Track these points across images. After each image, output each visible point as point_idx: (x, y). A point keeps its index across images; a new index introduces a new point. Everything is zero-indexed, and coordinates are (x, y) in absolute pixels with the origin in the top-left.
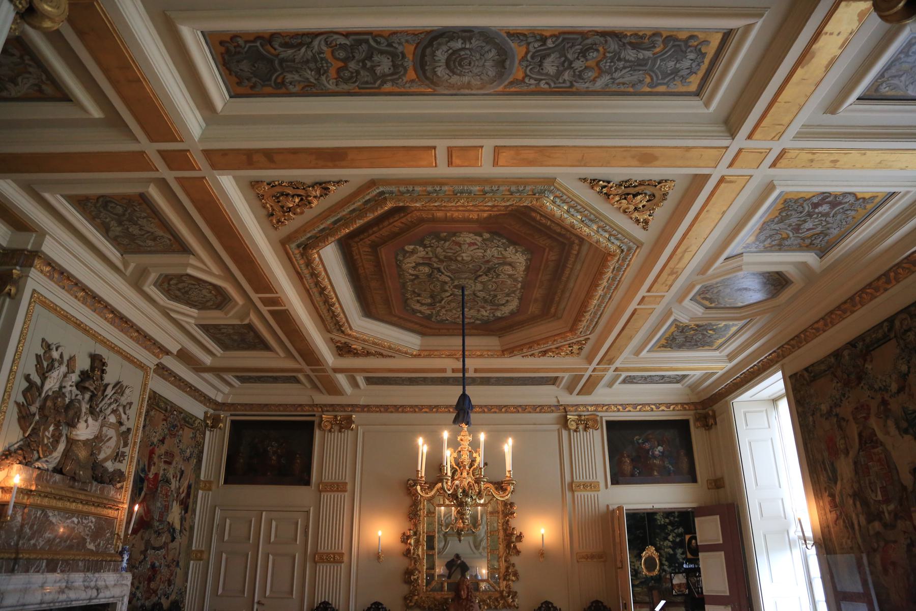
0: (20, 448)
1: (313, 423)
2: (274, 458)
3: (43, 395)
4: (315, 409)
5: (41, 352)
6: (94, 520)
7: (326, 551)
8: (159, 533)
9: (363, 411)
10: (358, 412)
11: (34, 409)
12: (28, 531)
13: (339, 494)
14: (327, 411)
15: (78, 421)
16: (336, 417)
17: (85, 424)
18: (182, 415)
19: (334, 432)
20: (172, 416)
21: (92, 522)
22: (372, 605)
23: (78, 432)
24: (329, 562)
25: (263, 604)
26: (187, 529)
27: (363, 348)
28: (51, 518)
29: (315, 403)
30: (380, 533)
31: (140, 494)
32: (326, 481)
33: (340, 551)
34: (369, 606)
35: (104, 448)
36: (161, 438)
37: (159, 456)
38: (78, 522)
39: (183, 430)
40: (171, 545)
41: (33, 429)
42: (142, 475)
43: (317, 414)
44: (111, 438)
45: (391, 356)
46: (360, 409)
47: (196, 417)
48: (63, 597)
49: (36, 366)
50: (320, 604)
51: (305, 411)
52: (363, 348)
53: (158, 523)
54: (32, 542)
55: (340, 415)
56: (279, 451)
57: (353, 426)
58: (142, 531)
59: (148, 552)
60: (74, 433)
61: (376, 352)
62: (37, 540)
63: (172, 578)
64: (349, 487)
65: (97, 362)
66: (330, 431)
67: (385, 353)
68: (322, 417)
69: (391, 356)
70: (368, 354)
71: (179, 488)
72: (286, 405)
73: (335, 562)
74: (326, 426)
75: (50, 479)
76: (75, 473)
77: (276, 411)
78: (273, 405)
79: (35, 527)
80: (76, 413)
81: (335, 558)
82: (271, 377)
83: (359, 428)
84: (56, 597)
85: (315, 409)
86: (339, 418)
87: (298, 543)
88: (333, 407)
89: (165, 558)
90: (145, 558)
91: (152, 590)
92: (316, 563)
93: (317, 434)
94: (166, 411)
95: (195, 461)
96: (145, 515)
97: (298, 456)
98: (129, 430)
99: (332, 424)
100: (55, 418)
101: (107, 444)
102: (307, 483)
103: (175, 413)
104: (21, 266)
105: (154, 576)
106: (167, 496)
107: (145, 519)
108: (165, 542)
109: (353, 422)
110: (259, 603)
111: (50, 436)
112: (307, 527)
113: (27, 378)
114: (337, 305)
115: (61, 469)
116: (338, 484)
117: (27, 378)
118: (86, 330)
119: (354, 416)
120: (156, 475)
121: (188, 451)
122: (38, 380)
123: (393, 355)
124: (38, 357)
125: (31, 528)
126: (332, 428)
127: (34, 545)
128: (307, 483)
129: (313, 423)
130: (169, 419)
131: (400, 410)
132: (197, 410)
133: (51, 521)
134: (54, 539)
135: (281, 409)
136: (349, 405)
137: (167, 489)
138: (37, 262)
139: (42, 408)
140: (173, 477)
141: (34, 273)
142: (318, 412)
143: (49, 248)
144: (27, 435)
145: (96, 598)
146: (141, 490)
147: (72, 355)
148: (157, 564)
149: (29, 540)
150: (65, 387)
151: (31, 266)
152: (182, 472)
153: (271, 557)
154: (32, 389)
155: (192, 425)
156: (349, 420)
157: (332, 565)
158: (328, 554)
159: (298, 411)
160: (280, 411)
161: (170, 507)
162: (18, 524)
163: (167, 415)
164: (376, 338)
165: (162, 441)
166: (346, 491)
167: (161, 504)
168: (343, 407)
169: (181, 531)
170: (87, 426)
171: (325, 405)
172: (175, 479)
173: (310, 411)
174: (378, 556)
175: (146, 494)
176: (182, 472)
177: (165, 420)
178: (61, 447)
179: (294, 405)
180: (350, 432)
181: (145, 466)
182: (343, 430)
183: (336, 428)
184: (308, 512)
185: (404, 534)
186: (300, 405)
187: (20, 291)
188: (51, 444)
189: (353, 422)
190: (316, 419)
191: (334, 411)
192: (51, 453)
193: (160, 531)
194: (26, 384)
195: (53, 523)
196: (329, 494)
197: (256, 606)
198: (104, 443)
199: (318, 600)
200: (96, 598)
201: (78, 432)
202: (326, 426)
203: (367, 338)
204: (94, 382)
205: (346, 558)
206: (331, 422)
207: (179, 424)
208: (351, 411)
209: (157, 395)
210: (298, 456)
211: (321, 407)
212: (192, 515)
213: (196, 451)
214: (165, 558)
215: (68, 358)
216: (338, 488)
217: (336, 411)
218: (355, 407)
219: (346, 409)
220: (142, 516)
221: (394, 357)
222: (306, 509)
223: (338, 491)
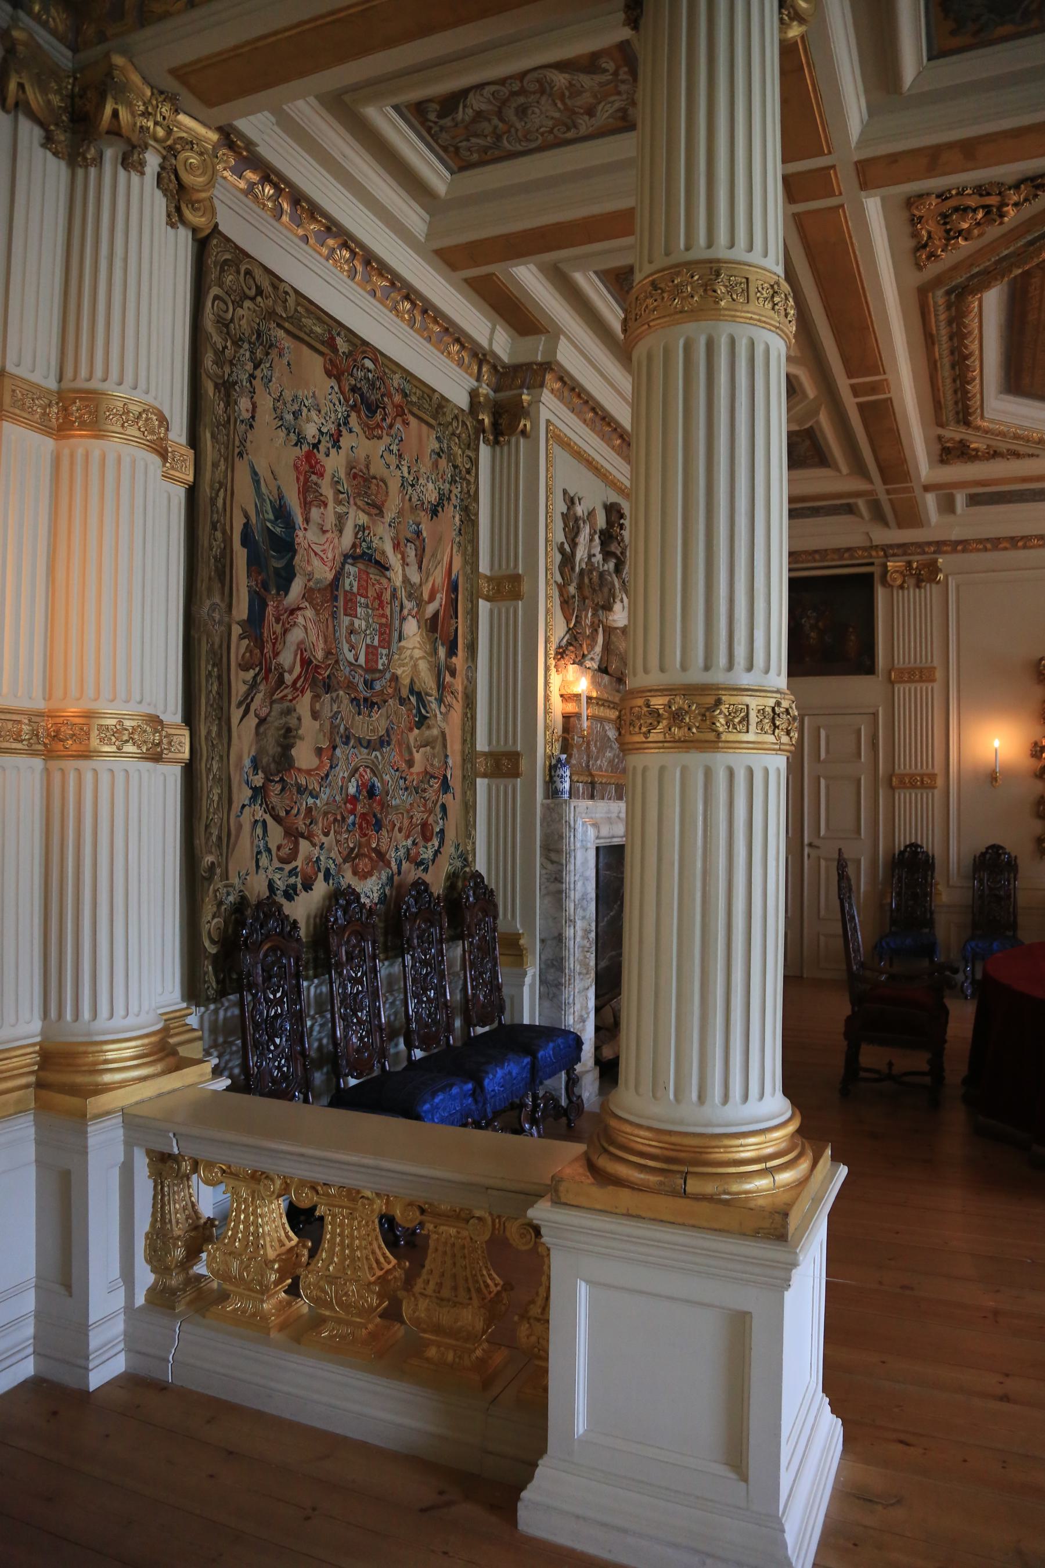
0: (569, 644)
1: (871, 575)
2: (812, 634)
3: (577, 569)
4: (874, 553)
7: (908, 770)
9: (954, 550)
10: (946, 552)
13: (924, 685)
14: (894, 555)
15: (614, 601)
16: (909, 564)
17: (621, 604)
19: (908, 588)
22: (987, 849)
23: (616, 617)
24: (914, 787)
25: (818, 847)
27: (988, 446)
29: (874, 543)
30: (997, 743)
32: (901, 665)
33: (930, 770)
34: (984, 850)
41: (577, 617)
43: (876, 561)
45: (1032, 455)
46: (949, 549)
49: (564, 529)
50: (906, 847)
51: (857, 559)
52: (988, 446)
55: (916, 560)
56: (820, 624)
57: (941, 576)
60: (610, 618)
61: (1008, 450)
62: (601, 761)
64: (939, 674)
66: (901, 587)
67: (1022, 450)
68: (886, 566)
69: (1032, 455)
70: (995, 454)
72: (826, 550)
73: (923, 786)
74: (895, 580)
76: (622, 673)
77: (808, 561)
78: (805, 552)
80: (610, 590)
81: (922, 782)
82: (809, 508)
83: (950, 579)
85: (874, 553)
86: (915, 565)
87: (863, 759)
88: (904, 548)
92: (892, 788)
93: (881, 594)
97: (851, 630)
99: (904, 576)
100: (593, 600)
102: (869, 669)
104: (528, 389)
109: (941, 571)
110: (810, 845)
112: (874, 737)
114: (977, 381)
115: (606, 668)
116: (921, 670)
119: (940, 560)
123: (1036, 452)
126: (904, 582)
128: (869, 669)
129: (871, 575)
131: (1020, 544)
135: (817, 557)
136: (929, 544)
138: (548, 377)
139: (580, 587)
141: (547, 396)
142: (878, 557)
143: (567, 356)
144: (572, 626)
147: (590, 510)
150: (594, 555)
151: (542, 385)
153: (823, 782)
156: (933, 569)
157: (919, 792)
158: (912, 776)
159: (846, 559)
160: (815, 561)
164: (1021, 427)
166: (933, 681)
168: (920, 547)
171: (891, 546)
173: (864, 558)
174: (992, 777)
179: (839, 550)
180: (934, 586)
182: (924, 584)
183: (912, 581)
184: (875, 715)
185: (1036, 744)
186: (848, 549)
187: (535, 425)
189: (941, 571)
190: (876, 570)
191: (905, 554)
196: (907, 686)
197: (806, 850)
199: (902, 841)
201: (616, 617)
202: (895, 580)
203: (1006, 429)
204: (619, 544)
205: (940, 782)
206: (902, 573)
208: (935, 552)
210: (851, 630)
211: (883, 550)
216: (921, 677)
217: (910, 555)
218: (939, 546)
219: (927, 549)
221: (1038, 456)
222: (871, 710)
223: (921, 680)
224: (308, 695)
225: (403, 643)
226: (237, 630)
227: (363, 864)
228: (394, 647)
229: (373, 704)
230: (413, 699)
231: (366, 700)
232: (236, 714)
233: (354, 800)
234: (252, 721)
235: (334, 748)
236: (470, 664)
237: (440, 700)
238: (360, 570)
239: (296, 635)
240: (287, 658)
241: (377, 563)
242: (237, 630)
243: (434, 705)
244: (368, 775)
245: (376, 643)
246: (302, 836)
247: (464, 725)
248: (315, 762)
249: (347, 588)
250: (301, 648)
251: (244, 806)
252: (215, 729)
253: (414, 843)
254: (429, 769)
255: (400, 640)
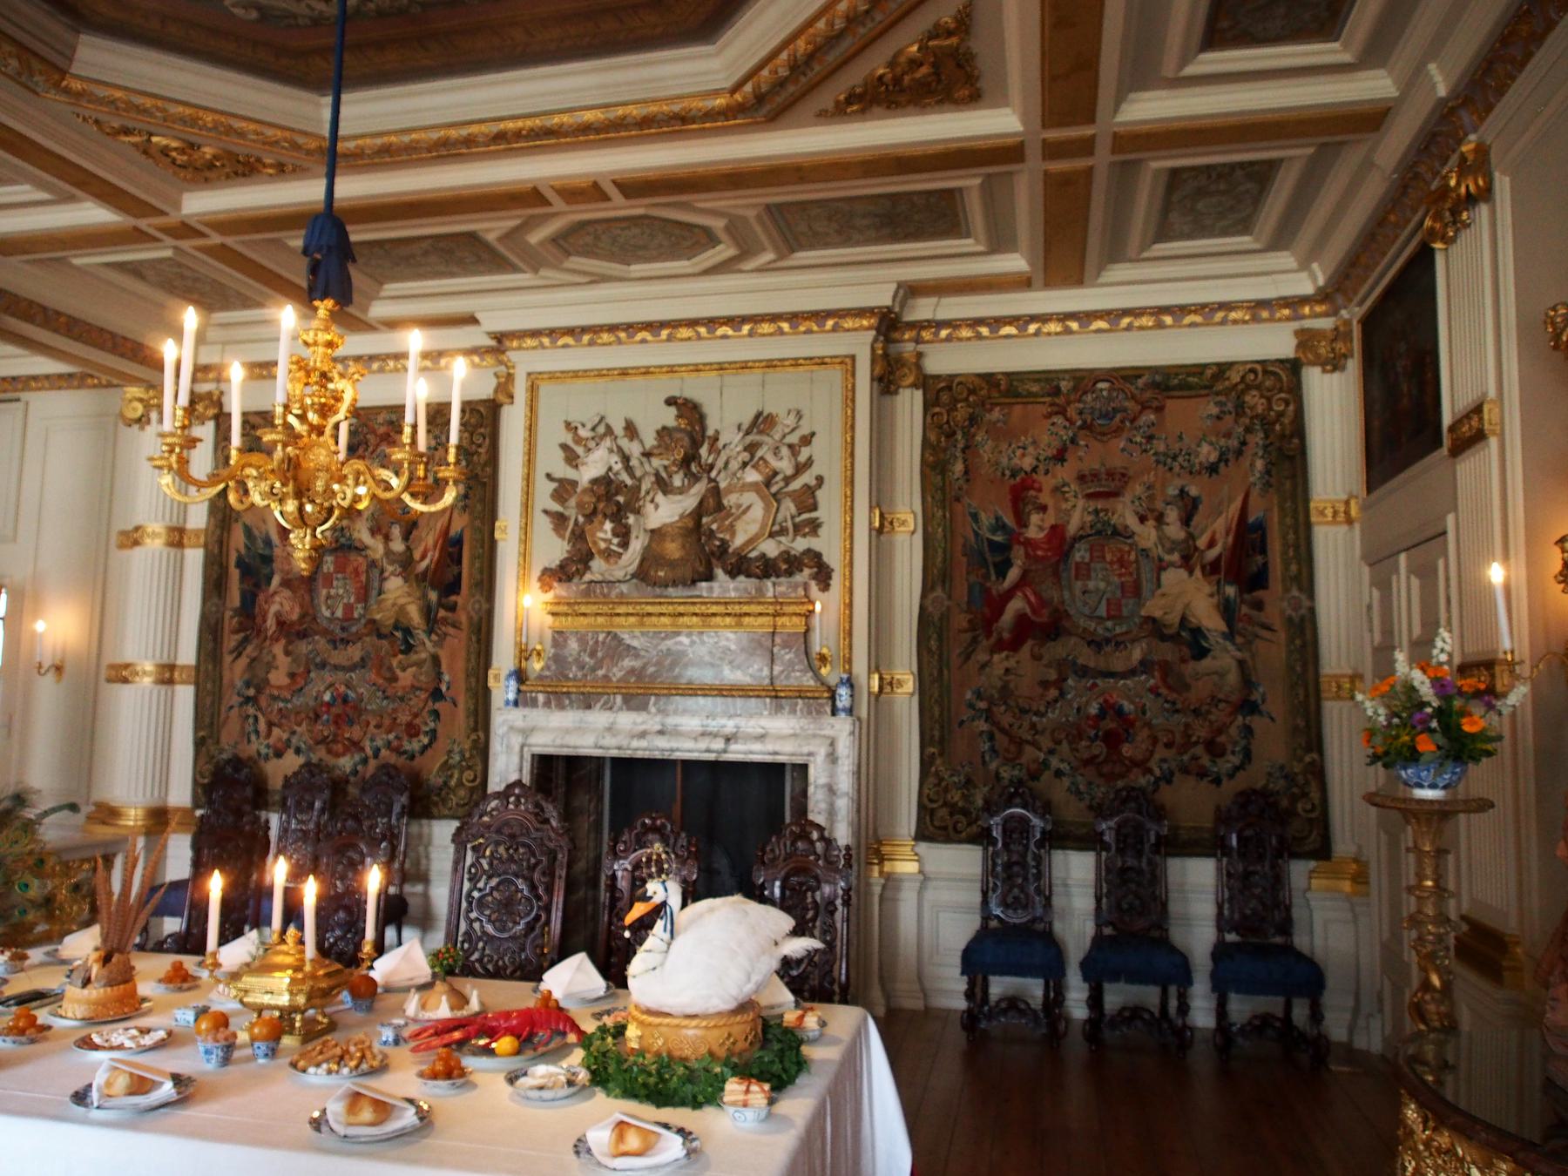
5: (568, 439)
6: (732, 636)
8: (1118, 644)
11: (571, 512)
12: (587, 659)
18: (1140, 382)
20: (1089, 398)
21: (727, 639)
26: (1277, 624)
28: (628, 641)
31: (1002, 574)
35: (739, 526)
36: (1050, 452)
37: (1057, 490)
38: (693, 643)
39: (1159, 410)
40: (1191, 668)
42: (998, 538)
44: (749, 508)
47: (1218, 365)
48: (635, 743)
53: (1109, 624)
54: (601, 673)
58: (1029, 643)
59: (1070, 682)
62: (608, 670)
63: (1222, 739)
65: (689, 410)
71: (1191, 537)
75: (609, 593)
79: (600, 654)
84: (625, 743)
89: (1158, 695)
90: (1062, 694)
91: (1131, 760)
94: (1056, 391)
95: (1259, 464)
96: (1034, 611)
98: (820, 480)
101: (745, 517)
103: (1101, 385)
105: (1127, 731)
106: (1122, 562)
107: (1033, 618)
108: (1142, 662)
111: (609, 535)
113: (549, 476)
117: (549, 476)
118: (646, 372)
120: (1057, 531)
121: (1205, 448)
122: (570, 473)
124: (564, 447)
125: (593, 654)
127: (606, 677)
130: (1072, 411)
132: (1275, 342)
133: (629, 646)
134: (644, 667)
137: (1120, 550)
140: (1142, 519)
145: (725, 751)
146: (1002, 568)
148: (1128, 707)
149: (593, 670)
152: (1189, 508)
154: (564, 489)
155: (1210, 387)
161: (1146, 587)
162: (575, 653)
163: (1060, 400)
165: (1060, 457)
167: (1109, 583)
169: (1230, 636)
170: (657, 507)
172: (1151, 523)
175: (1025, 574)
176: (1189, 508)
177: (1062, 412)
178: (637, 545)
181: (997, 519)
188: (619, 545)
192: (620, 555)
193: (1120, 639)
194: (555, 485)
195: (635, 648)
198: (738, 518)
200: (725, 751)
207: (1129, 404)
209: (1000, 377)
212: (1287, 590)
213: (1258, 438)
214: (1158, 695)
215: (624, 424)
220: (1025, 614)
224: (283, 642)
225: (383, 596)
226: (228, 614)
227: (339, 747)
228: (372, 601)
229: (348, 642)
230: (398, 634)
231: (342, 640)
232: (228, 659)
233: (328, 705)
234: (243, 662)
235: (309, 672)
236: (478, 597)
237: (430, 632)
238: (337, 557)
239: (274, 608)
240: (271, 623)
241: (356, 548)
242: (228, 614)
243: (423, 636)
244: (342, 689)
245: (352, 600)
246: (275, 725)
247: (469, 647)
248: (286, 681)
249: (325, 570)
250: (278, 615)
251: (231, 707)
252: (210, 667)
253: (397, 738)
254: (416, 684)
255: (380, 594)
